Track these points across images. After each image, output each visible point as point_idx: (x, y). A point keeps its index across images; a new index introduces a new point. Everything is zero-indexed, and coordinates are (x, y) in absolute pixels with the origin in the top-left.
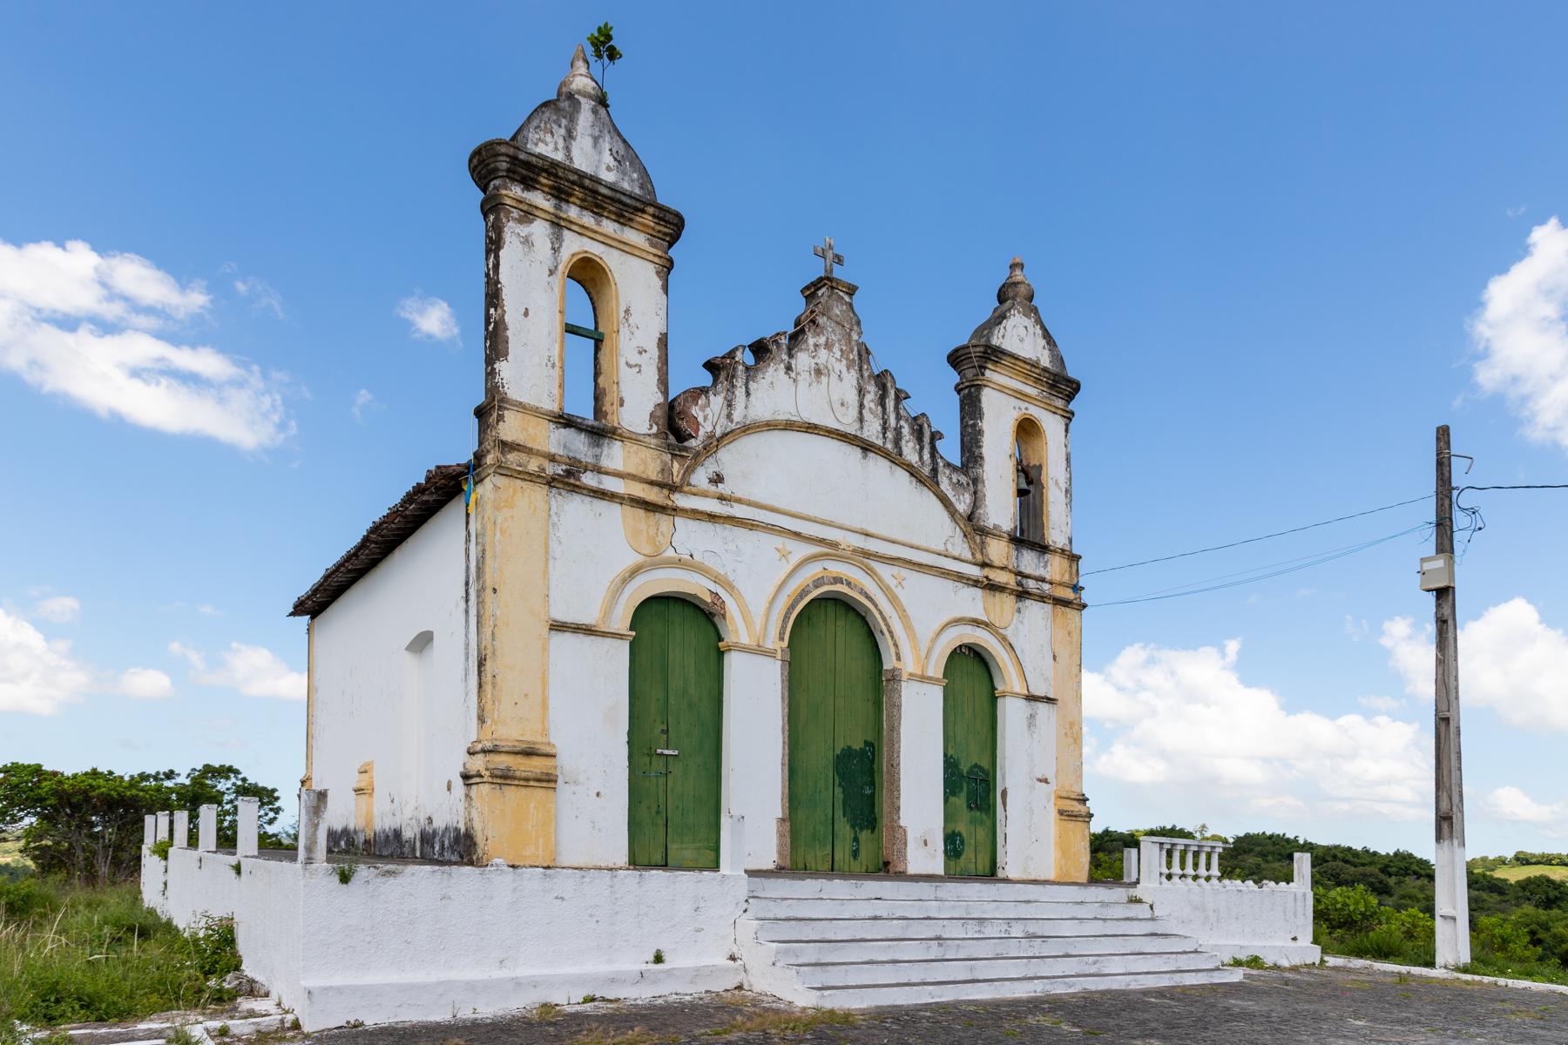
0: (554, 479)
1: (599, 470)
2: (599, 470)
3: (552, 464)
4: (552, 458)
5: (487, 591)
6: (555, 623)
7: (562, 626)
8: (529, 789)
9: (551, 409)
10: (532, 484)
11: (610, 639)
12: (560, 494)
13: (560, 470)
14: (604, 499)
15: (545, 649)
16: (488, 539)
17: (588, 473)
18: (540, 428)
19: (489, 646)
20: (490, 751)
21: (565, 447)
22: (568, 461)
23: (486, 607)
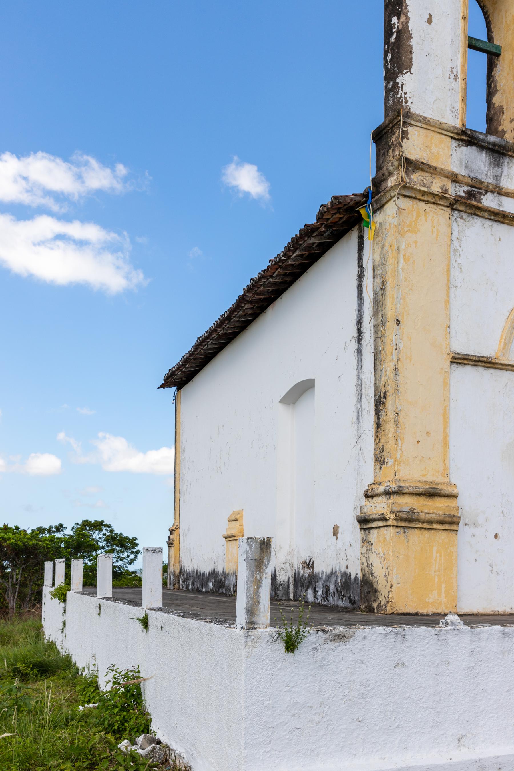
0: (457, 201)
1: (500, 192)
2: (500, 192)
3: (454, 185)
4: (455, 179)
5: (388, 324)
6: (456, 356)
7: (464, 359)
8: (433, 531)
9: (453, 124)
10: (435, 206)
11: (508, 372)
12: (462, 218)
13: (461, 191)
14: (503, 223)
15: (446, 384)
16: (389, 269)
17: (489, 195)
18: (443, 145)
19: (391, 382)
20: (394, 493)
21: (466, 166)
22: (470, 181)
23: (387, 341)
